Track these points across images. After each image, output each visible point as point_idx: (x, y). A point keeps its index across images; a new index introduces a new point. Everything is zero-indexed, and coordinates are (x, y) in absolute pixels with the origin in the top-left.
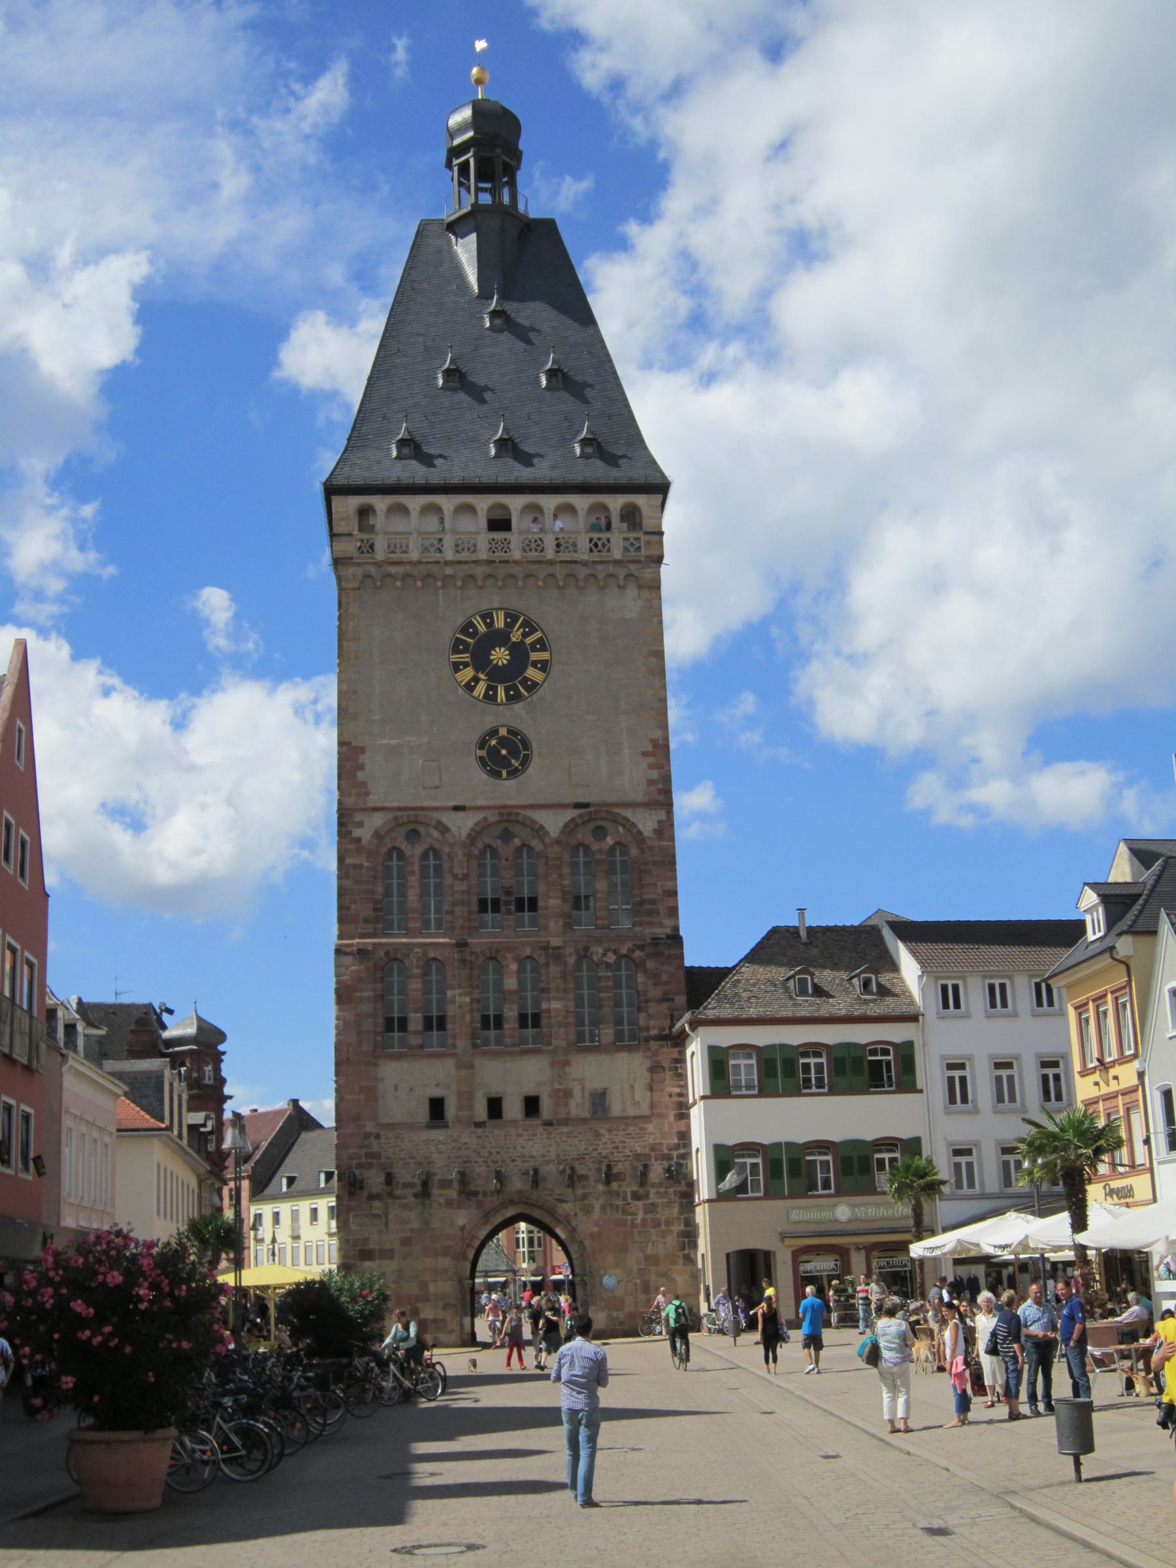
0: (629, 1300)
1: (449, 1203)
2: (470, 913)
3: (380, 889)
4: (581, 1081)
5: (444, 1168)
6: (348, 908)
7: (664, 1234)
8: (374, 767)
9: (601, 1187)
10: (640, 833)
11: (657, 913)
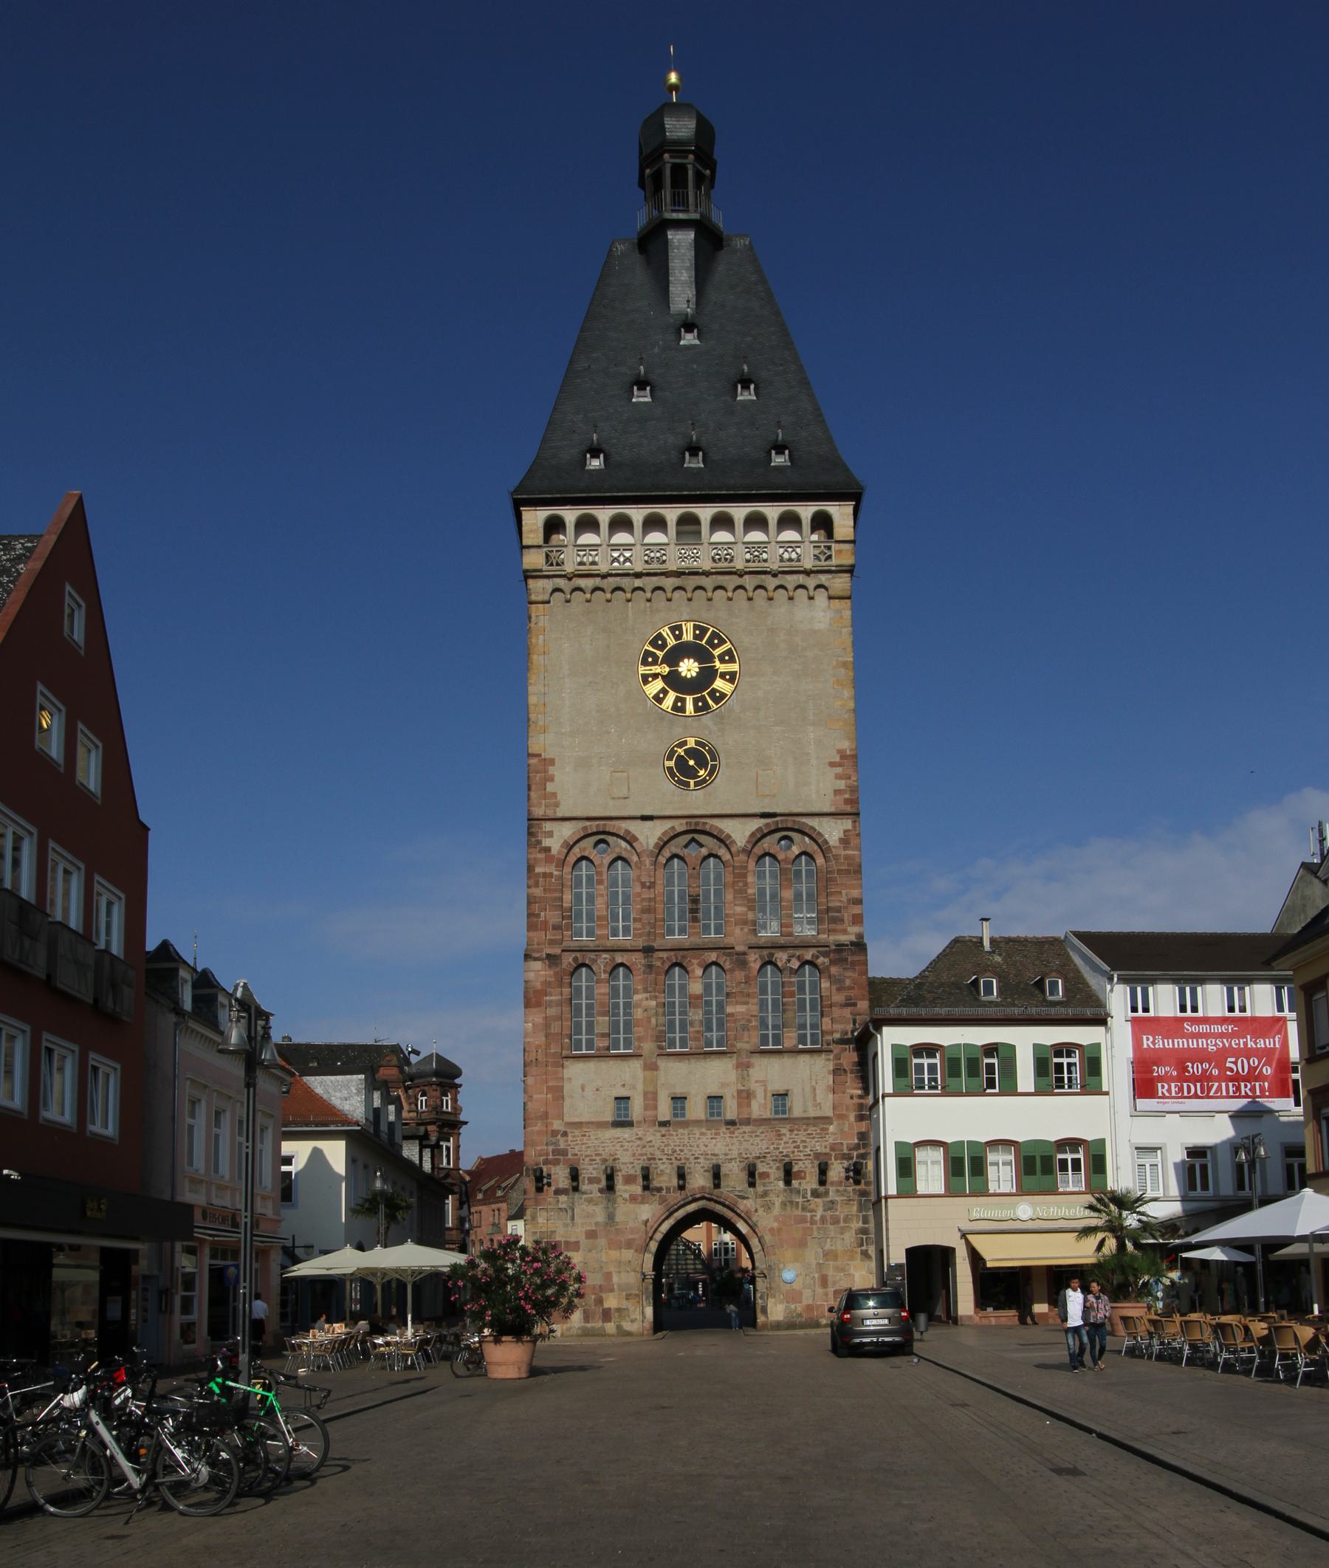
0: (807, 1294)
1: (633, 1199)
4: (764, 1083)
5: (628, 1164)
6: (538, 916)
7: (842, 1231)
9: (781, 1184)
10: (826, 842)
11: (842, 920)
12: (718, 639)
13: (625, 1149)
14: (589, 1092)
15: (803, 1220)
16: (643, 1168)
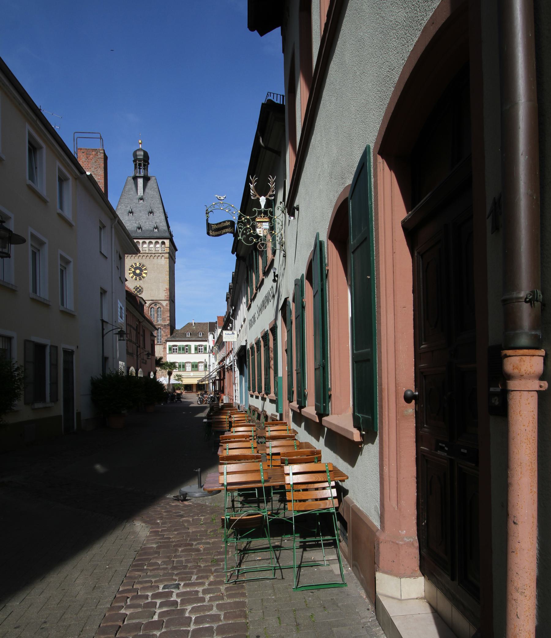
12: (143, 266)
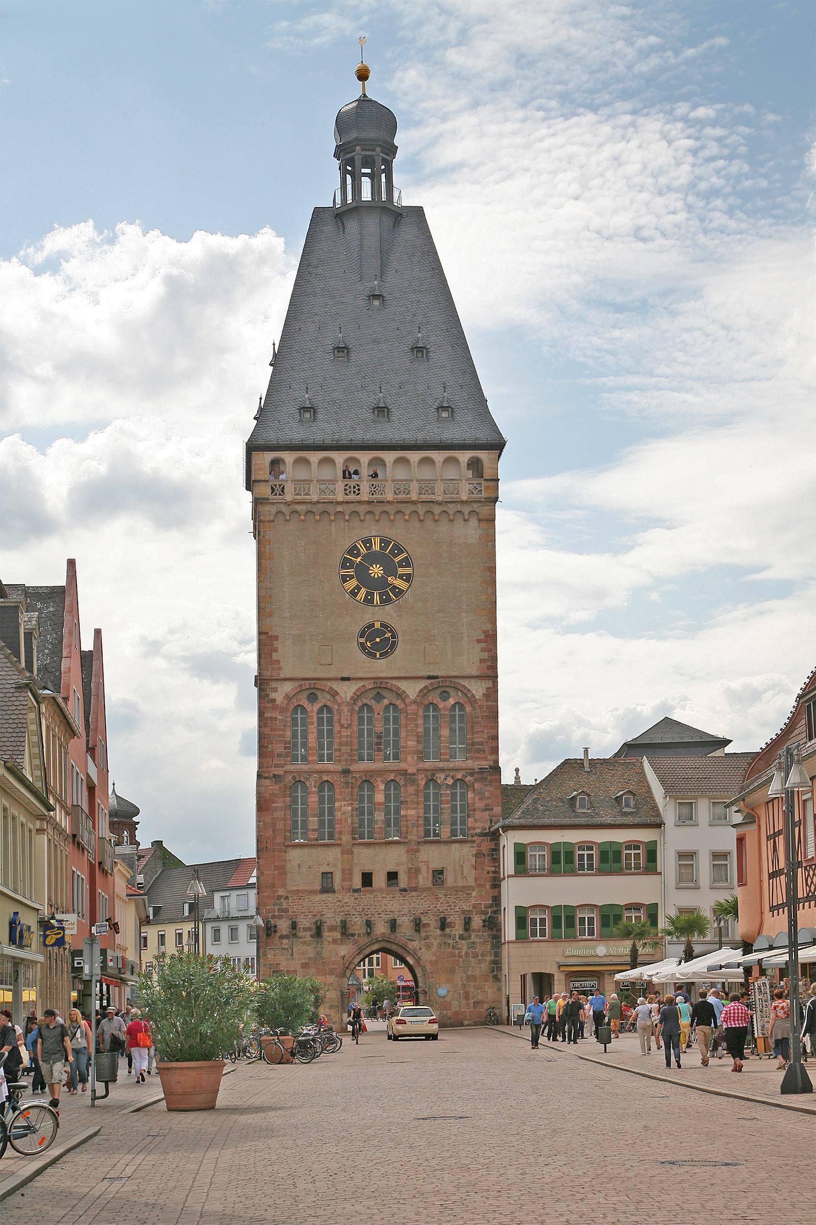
0: (455, 1003)
1: (335, 941)
2: (352, 750)
3: (289, 733)
4: (427, 863)
5: (332, 918)
7: (480, 962)
8: (285, 652)
9: (438, 932)
10: (473, 696)
13: (330, 908)
14: (304, 870)
15: (453, 955)
16: (342, 921)
